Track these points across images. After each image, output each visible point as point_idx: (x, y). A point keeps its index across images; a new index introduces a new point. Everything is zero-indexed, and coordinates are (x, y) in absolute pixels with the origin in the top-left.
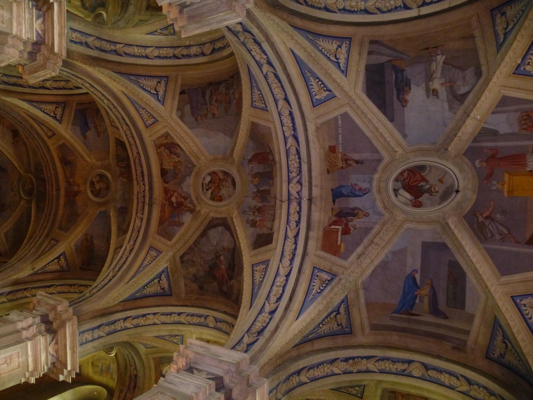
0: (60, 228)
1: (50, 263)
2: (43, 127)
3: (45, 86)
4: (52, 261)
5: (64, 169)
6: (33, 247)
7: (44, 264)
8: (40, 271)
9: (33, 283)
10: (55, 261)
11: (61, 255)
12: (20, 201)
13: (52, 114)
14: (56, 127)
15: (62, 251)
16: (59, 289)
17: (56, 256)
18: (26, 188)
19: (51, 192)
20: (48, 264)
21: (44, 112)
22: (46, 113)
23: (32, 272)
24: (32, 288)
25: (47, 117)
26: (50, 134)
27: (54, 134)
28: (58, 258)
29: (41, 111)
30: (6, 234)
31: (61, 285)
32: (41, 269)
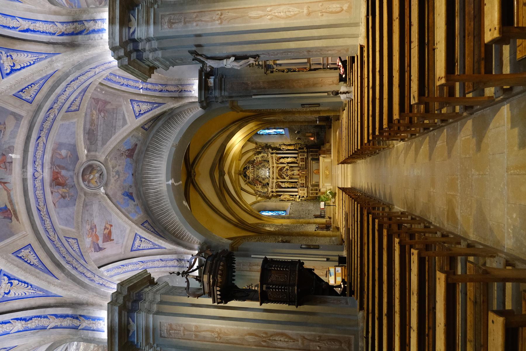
0: (18, 117)
1: (27, 66)
2: (35, 261)
3: (23, 322)
4: (24, 67)
5: (11, 202)
6: (59, 96)
7: (36, 65)
8: (43, 56)
9: (52, 41)
10: (19, 67)
11: (8, 74)
12: (106, 159)
13: (15, 282)
14: (8, 264)
15: (5, 79)
16: (13, 23)
17: (18, 73)
18: (97, 175)
19: (39, 169)
20: (30, 65)
21: (28, 284)
22: (25, 283)
23: (54, 58)
24: (54, 34)
25: (22, 278)
26: (23, 253)
27: (16, 253)
28: (13, 71)
29: (31, 285)
30: (125, 122)
31: (9, 28)
32: (39, 60)
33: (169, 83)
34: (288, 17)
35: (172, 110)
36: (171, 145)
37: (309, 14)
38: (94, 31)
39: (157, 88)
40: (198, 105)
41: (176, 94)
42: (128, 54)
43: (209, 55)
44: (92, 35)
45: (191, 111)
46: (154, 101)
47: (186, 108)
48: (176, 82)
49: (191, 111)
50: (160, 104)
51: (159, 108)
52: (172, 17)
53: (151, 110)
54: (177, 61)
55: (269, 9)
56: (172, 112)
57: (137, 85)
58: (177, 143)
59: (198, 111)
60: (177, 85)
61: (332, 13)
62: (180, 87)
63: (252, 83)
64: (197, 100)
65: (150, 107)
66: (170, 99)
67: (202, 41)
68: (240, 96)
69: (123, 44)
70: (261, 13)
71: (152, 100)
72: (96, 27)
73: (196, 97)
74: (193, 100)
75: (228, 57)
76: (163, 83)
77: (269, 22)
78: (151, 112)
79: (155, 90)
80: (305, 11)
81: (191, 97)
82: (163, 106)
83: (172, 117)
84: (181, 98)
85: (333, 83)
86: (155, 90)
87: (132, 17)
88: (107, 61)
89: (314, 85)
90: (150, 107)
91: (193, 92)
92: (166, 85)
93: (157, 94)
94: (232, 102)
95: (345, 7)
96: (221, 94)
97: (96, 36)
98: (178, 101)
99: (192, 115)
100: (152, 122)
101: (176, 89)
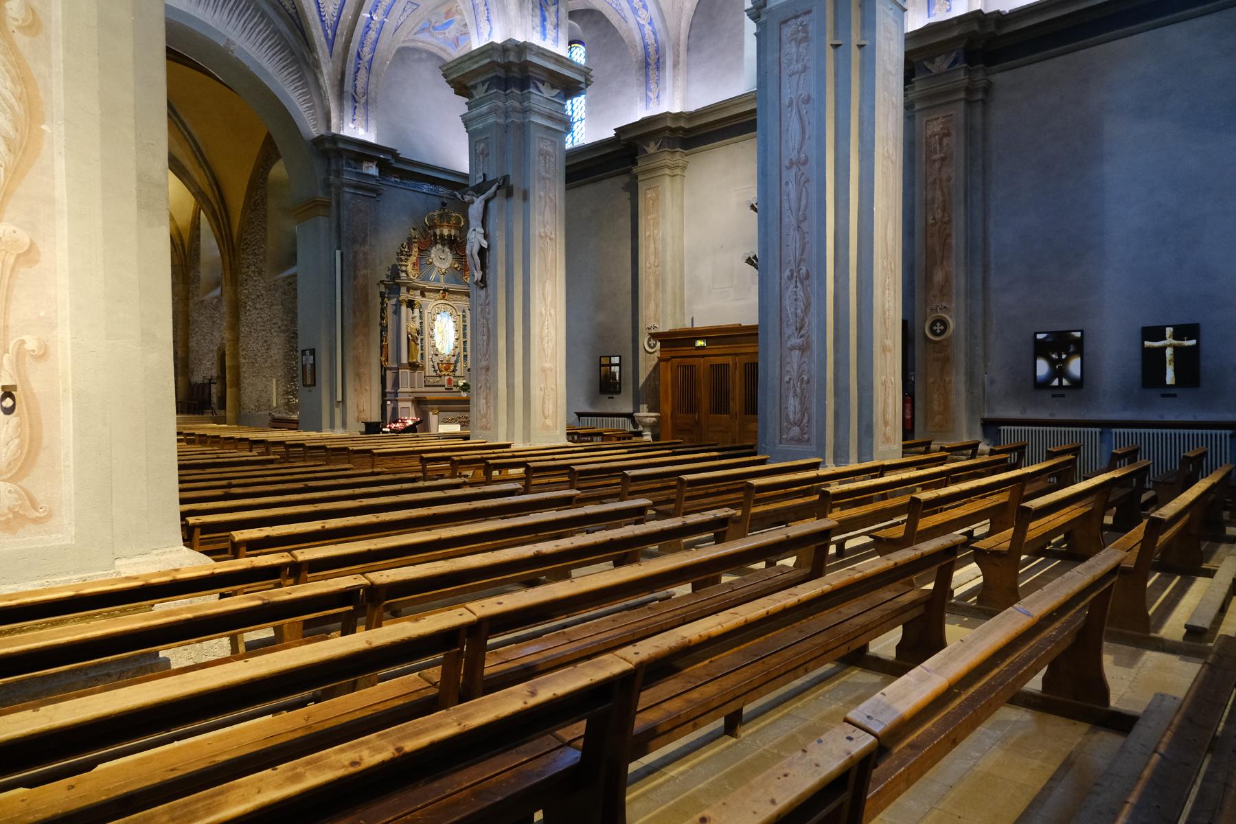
33: (373, 79)
34: (542, 339)
35: (315, 66)
36: (231, 38)
37: (544, 370)
38: (544, 19)
39: (366, 50)
40: (323, 131)
41: (348, 87)
42: (507, 66)
43: (491, 204)
44: (538, 12)
45: (310, 108)
46: (338, 32)
47: (315, 100)
48: (372, 94)
49: (310, 108)
50: (331, 44)
51: (323, 39)
52: (553, 160)
53: (322, 21)
54: (482, 145)
55: (553, 312)
56: (307, 63)
57: (380, 11)
58: (236, 54)
59: (313, 129)
60: (366, 93)
61: (544, 403)
62: (363, 100)
63: (365, 254)
64: (334, 130)
65: (329, 20)
66: (339, 70)
67: (517, 200)
68: (339, 225)
69: (525, 66)
70: (548, 301)
71: (342, 28)
72: (549, 26)
73: (340, 129)
74: (334, 121)
75: (486, 236)
76: (375, 65)
77: (537, 311)
78: (317, 18)
79: (362, 44)
80: (547, 365)
81: (341, 118)
82: (327, 51)
83: (295, 61)
84: (341, 95)
85: (360, 412)
86: (362, 44)
87: (556, 92)
88: (492, 17)
89: (358, 376)
90: (329, 20)
91: (351, 126)
92: (369, 71)
93: (354, 46)
94: (327, 205)
95: (549, 422)
96: (349, 185)
97: (538, 20)
98: (333, 86)
99: (302, 108)
100: (292, 11)
101: (359, 90)
